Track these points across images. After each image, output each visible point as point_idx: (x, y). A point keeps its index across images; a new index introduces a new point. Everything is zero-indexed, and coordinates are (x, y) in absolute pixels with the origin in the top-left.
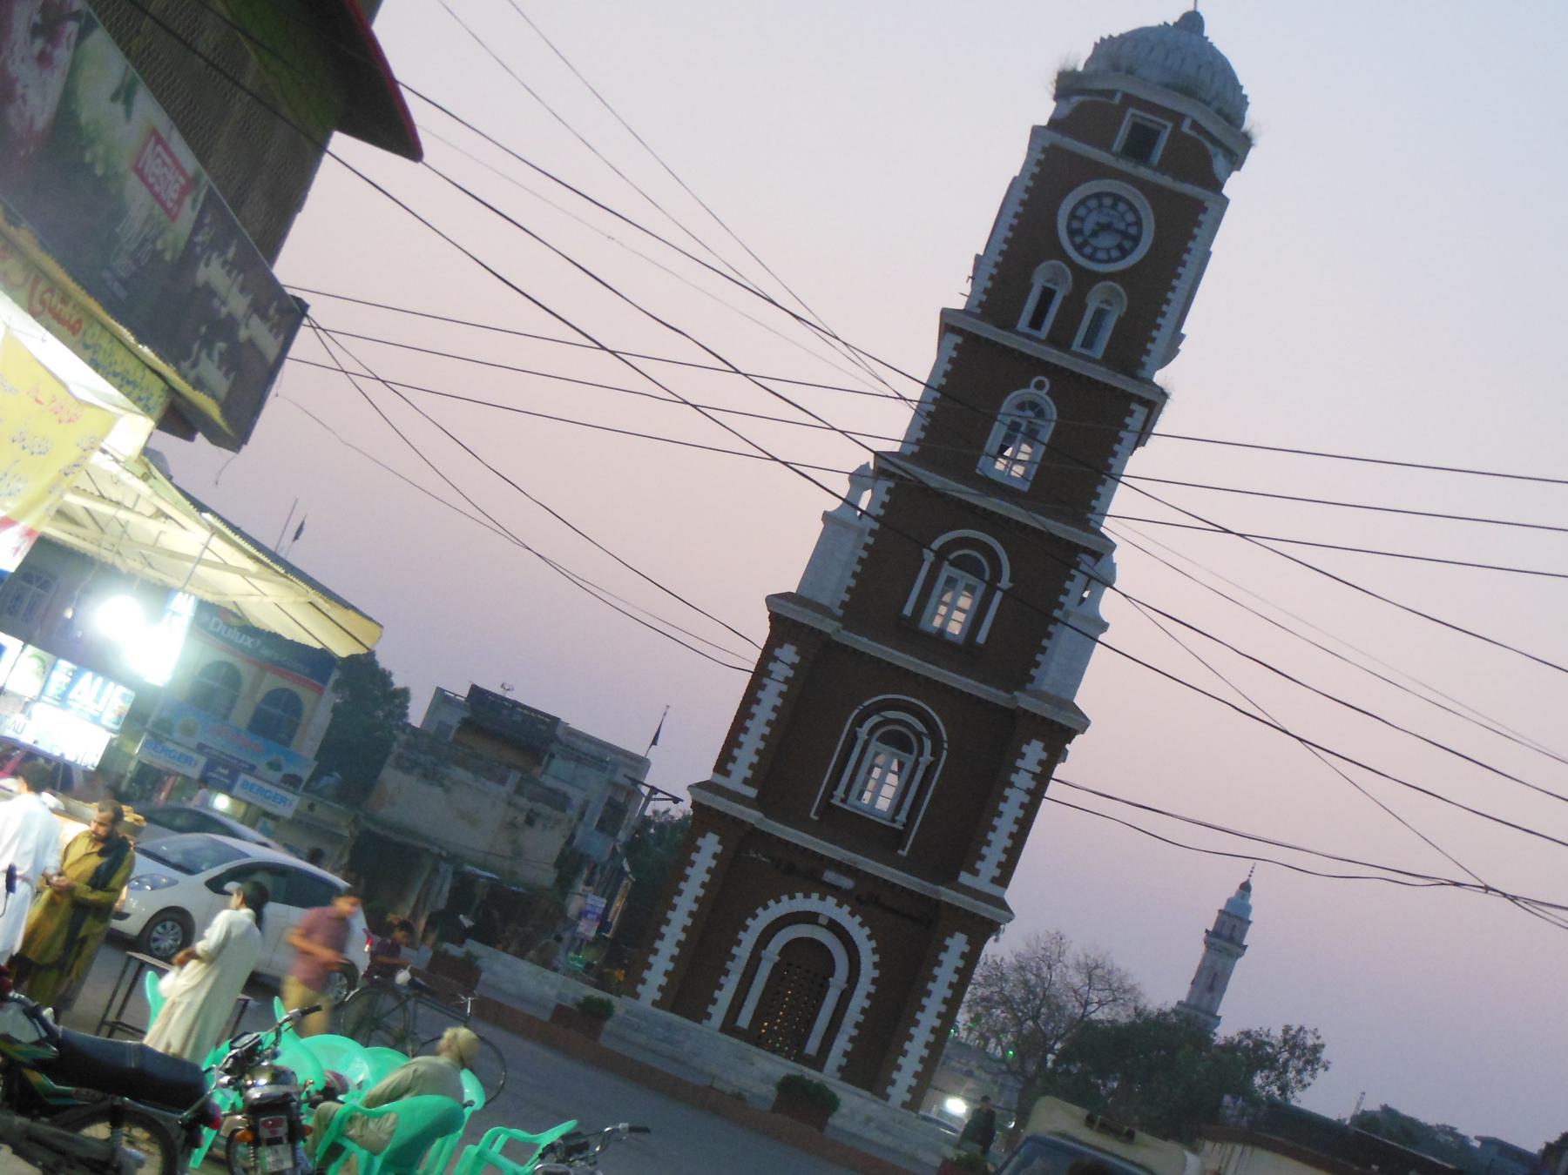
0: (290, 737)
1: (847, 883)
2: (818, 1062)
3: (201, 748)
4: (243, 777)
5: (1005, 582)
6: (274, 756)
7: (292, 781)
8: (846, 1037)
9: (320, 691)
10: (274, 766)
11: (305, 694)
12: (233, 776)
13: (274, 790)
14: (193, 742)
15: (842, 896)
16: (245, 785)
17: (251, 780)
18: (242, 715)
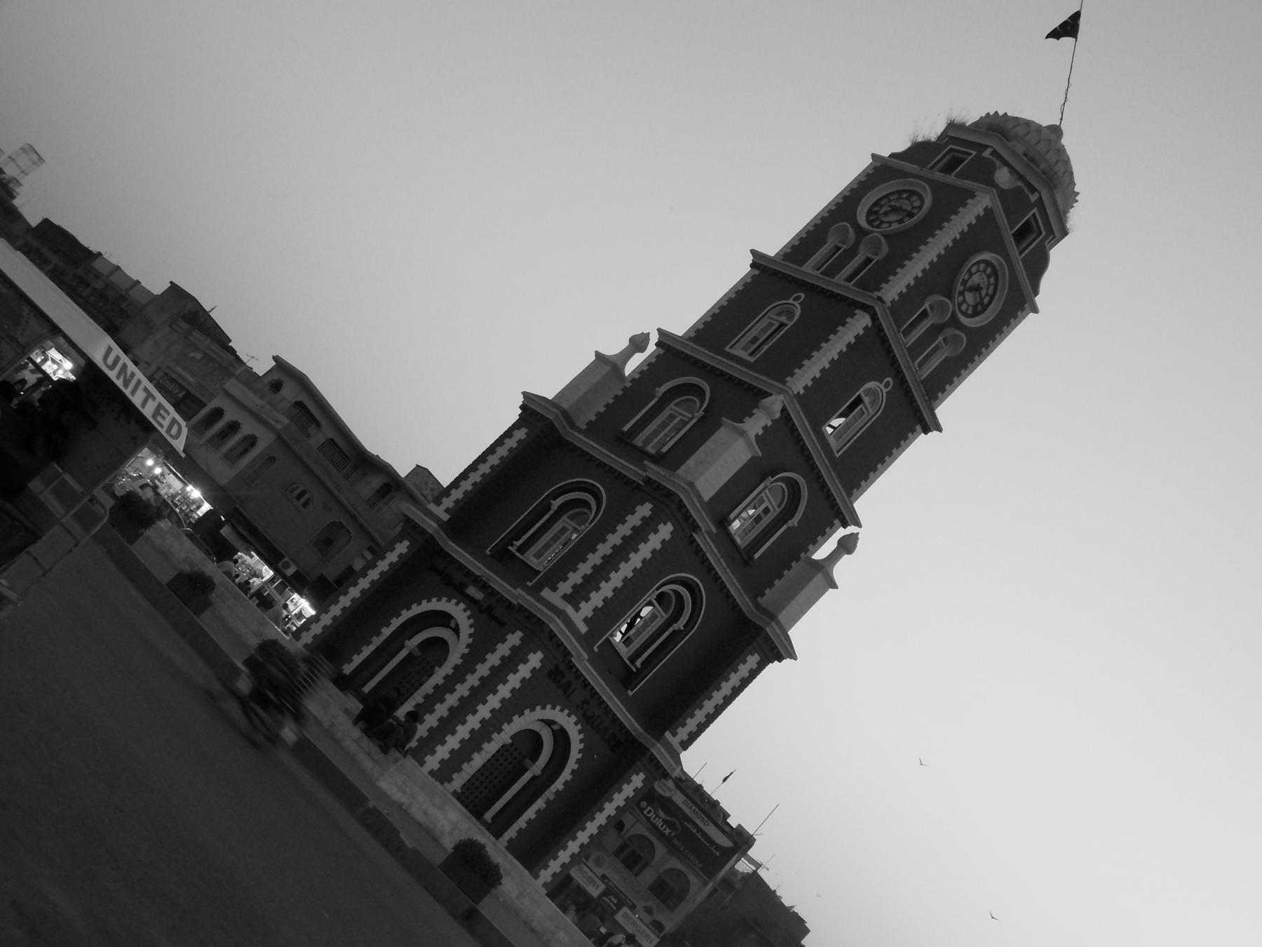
0: (676, 906)
1: (479, 596)
2: (497, 829)
3: (603, 878)
4: (625, 909)
5: (794, 522)
6: (650, 904)
7: (658, 926)
8: (472, 763)
9: (705, 884)
10: (649, 911)
11: (694, 881)
12: (620, 905)
13: (644, 927)
14: (600, 872)
15: (471, 601)
16: (625, 915)
17: (628, 911)
18: (648, 876)
